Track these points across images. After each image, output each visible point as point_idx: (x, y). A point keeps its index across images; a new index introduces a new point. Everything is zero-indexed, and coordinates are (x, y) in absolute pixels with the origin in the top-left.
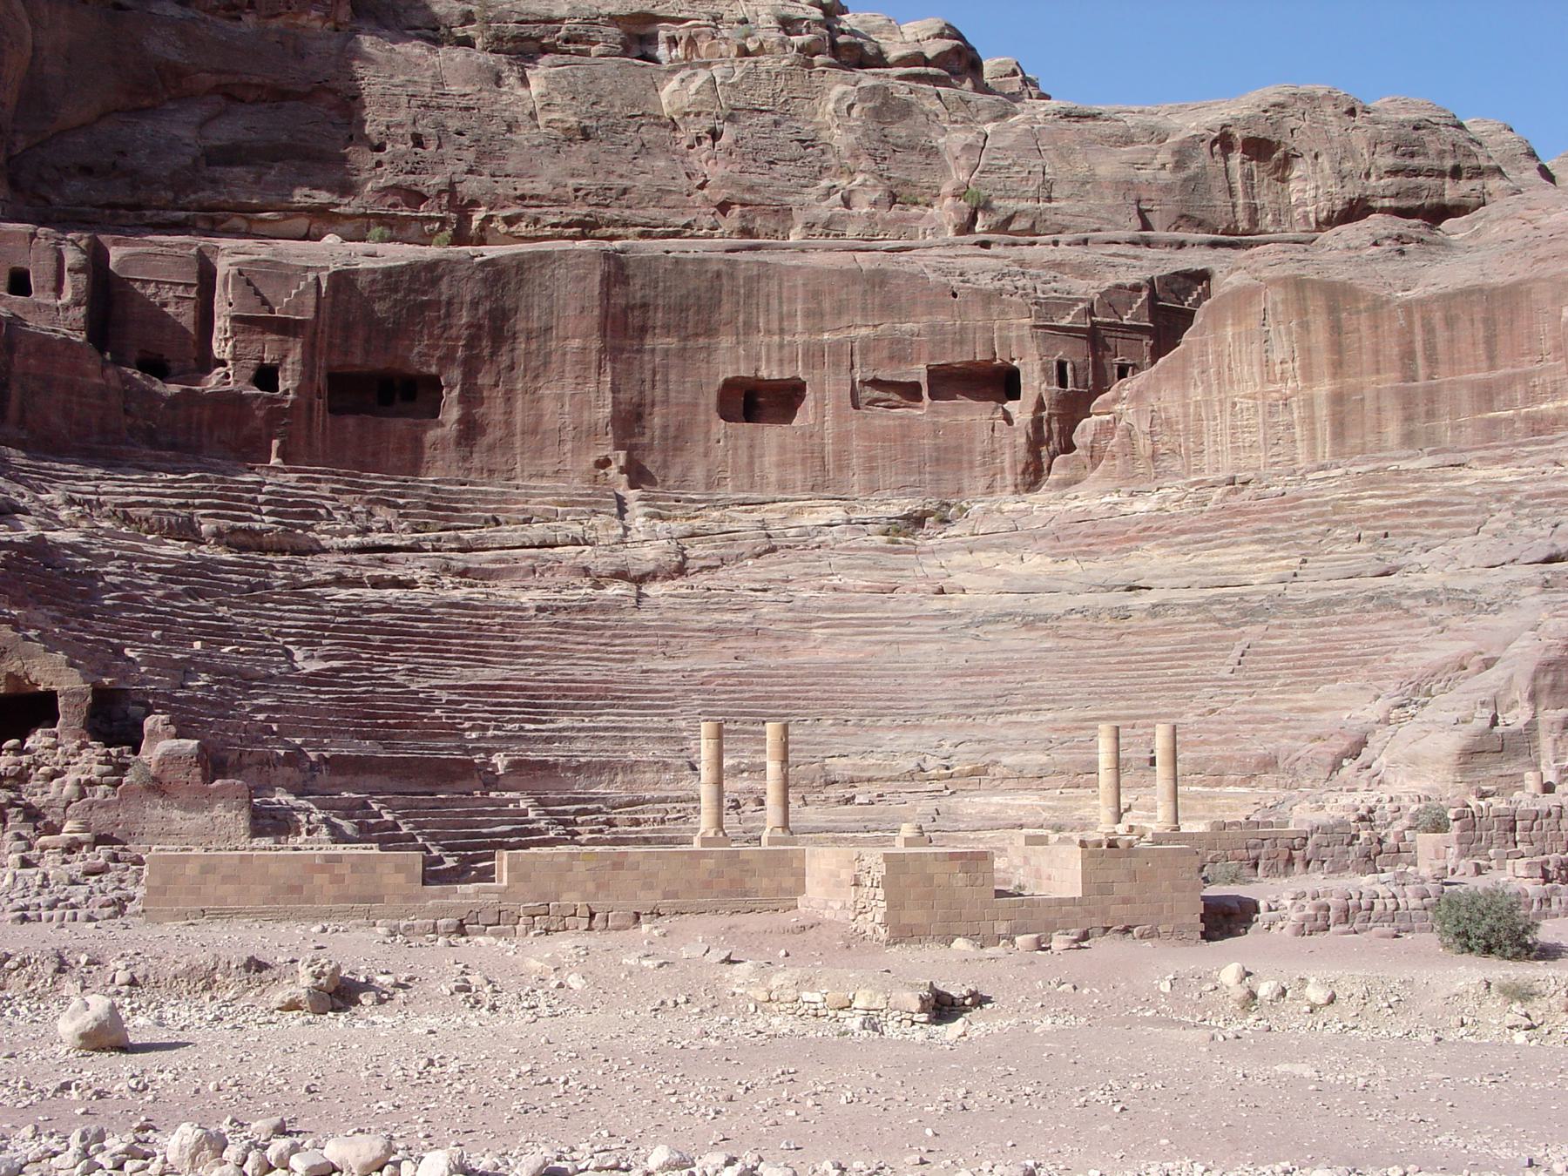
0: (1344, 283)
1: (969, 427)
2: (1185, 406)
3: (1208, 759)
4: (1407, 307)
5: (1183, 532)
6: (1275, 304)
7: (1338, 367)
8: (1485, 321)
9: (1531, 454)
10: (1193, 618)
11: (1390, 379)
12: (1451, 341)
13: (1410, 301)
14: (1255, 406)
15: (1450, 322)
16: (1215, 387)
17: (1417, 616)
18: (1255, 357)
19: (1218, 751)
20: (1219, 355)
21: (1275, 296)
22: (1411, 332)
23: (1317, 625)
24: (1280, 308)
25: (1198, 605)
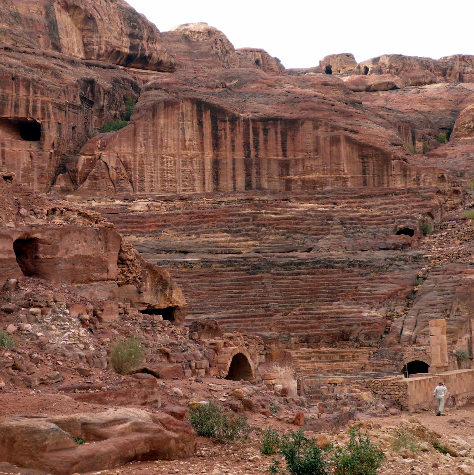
0: (219, 106)
1: (18, 154)
2: (135, 156)
3: (309, 335)
4: (246, 121)
5: (178, 224)
6: (187, 111)
7: (216, 145)
8: (282, 133)
9: (318, 199)
10: (229, 268)
11: (240, 155)
12: (266, 141)
13: (248, 119)
14: (175, 160)
15: (266, 132)
16: (151, 149)
17: (348, 272)
18: (176, 137)
19: (310, 332)
20: (156, 132)
21: (186, 107)
22: (249, 134)
23: (297, 274)
24: (189, 113)
25: (223, 262)
